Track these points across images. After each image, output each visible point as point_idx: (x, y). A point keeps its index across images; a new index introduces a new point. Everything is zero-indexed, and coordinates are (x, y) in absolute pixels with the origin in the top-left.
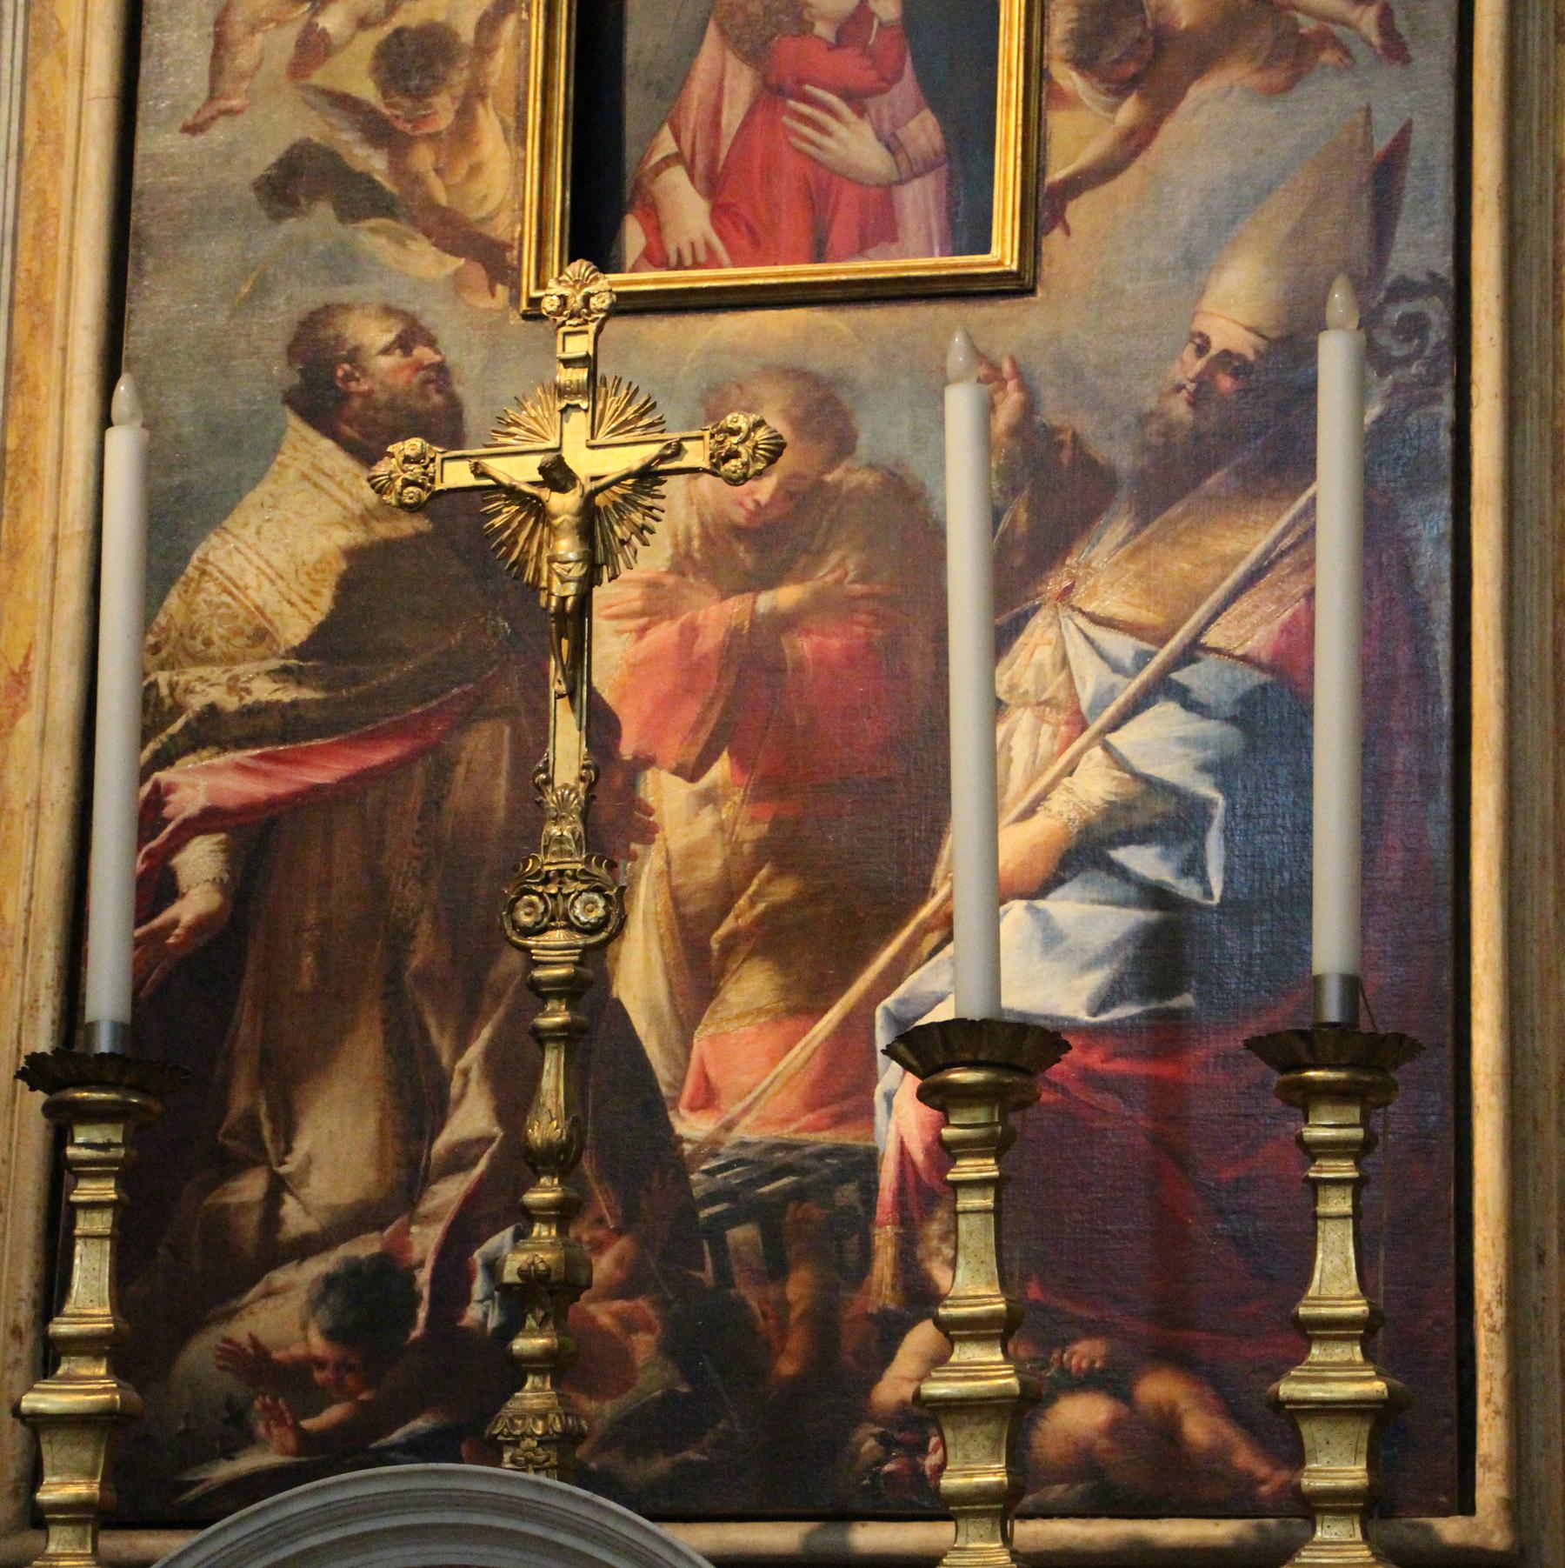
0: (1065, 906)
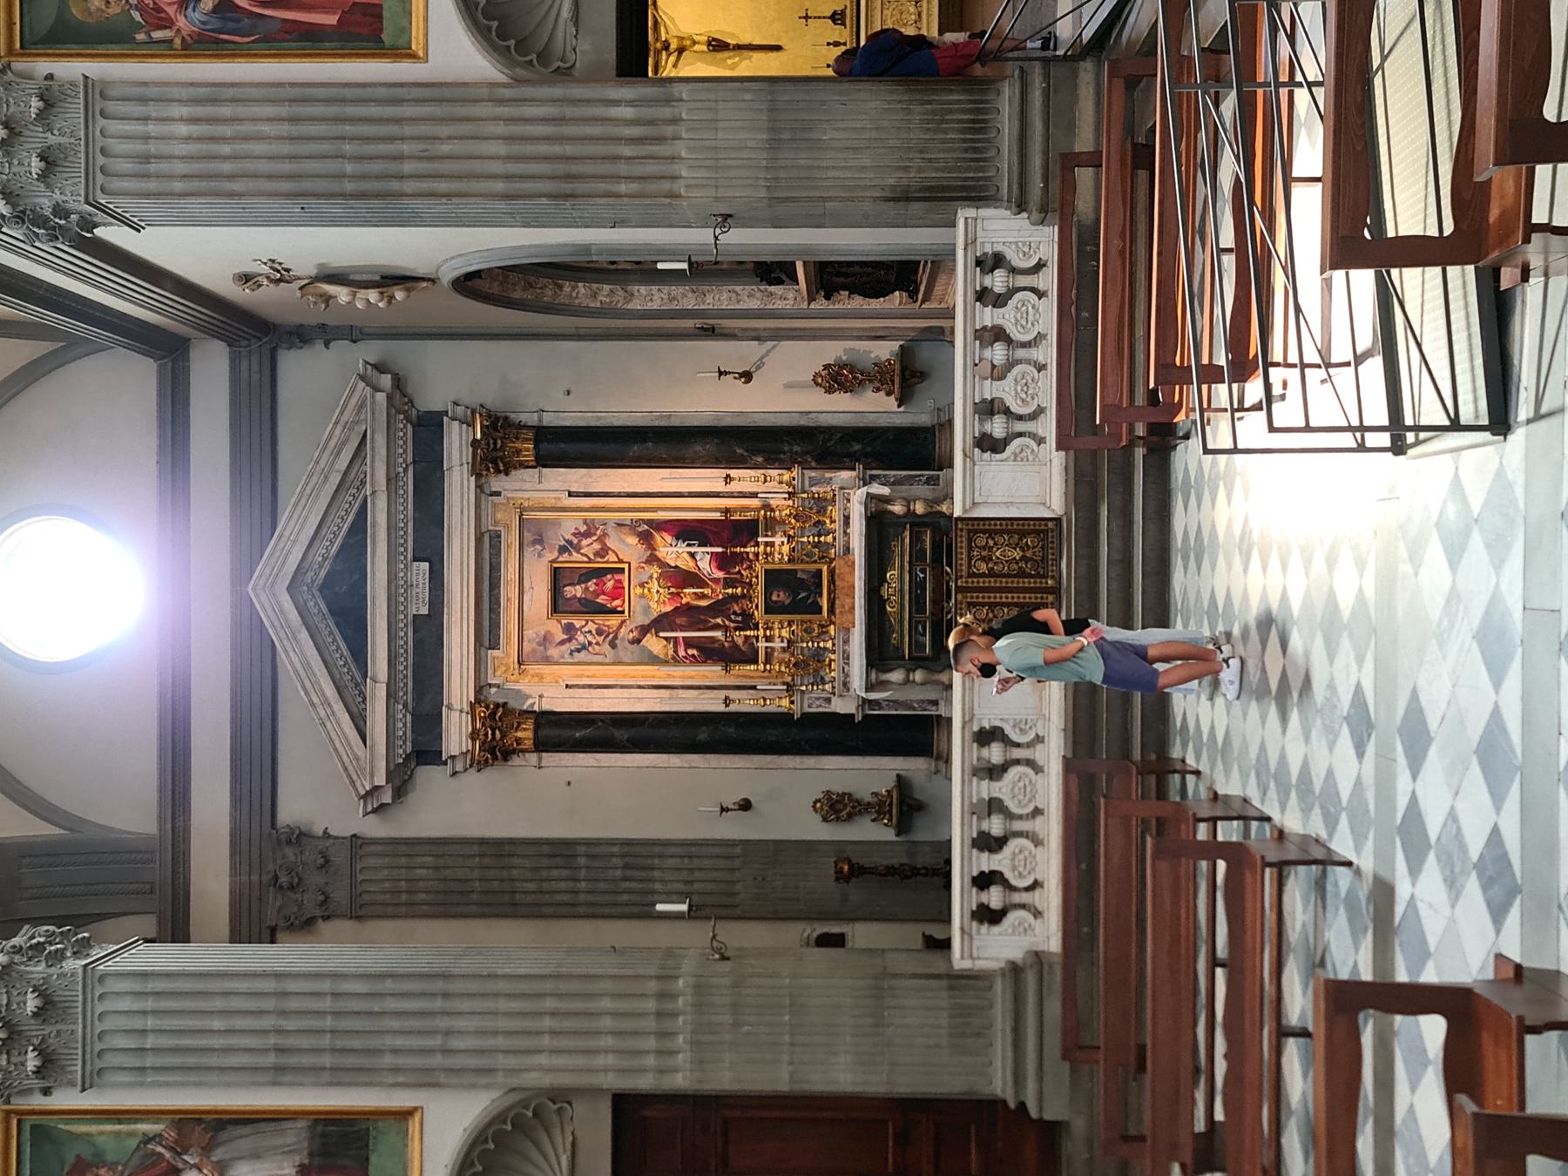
0: (698, 558)
